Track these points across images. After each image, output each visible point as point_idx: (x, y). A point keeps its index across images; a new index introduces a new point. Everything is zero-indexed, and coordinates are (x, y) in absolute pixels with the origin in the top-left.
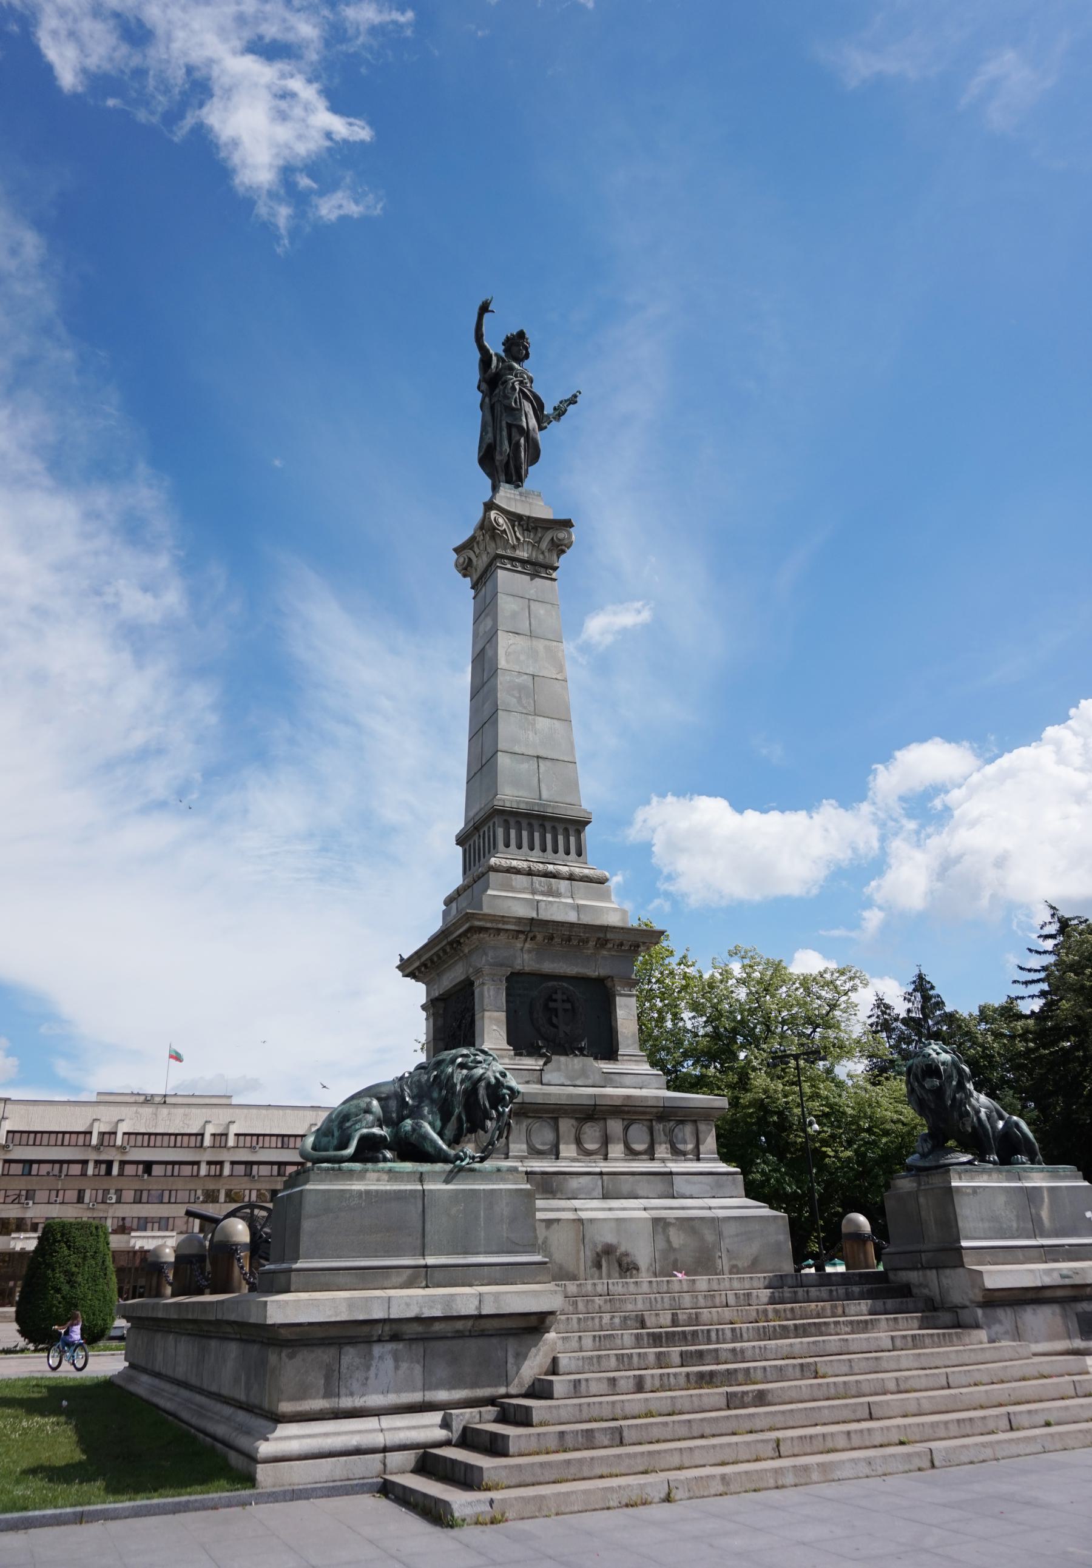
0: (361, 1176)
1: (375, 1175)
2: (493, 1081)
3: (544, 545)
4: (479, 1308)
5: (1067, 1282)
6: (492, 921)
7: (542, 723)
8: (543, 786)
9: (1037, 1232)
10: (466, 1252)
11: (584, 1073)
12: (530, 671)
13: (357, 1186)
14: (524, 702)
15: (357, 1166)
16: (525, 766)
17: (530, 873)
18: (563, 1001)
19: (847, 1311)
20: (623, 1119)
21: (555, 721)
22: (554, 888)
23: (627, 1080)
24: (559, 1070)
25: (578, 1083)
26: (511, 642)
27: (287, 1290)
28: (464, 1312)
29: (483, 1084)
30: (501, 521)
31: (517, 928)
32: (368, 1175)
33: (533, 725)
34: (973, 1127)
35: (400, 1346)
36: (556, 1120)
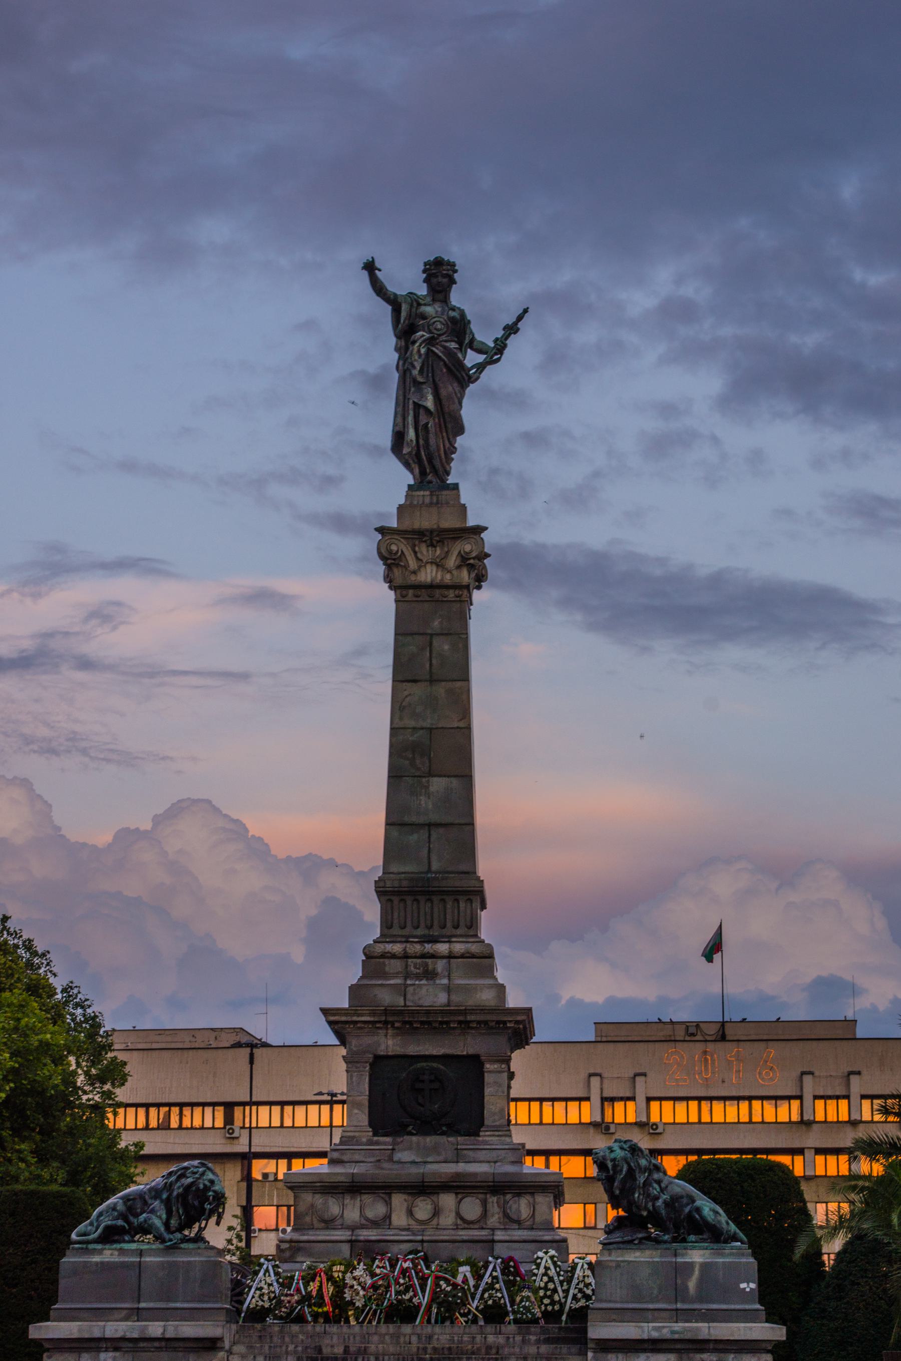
0: (100, 1252)
1: (110, 1252)
2: (201, 1186)
3: (452, 561)
4: (163, 1333)
5: (676, 1336)
6: (340, 1015)
7: (437, 784)
8: (434, 858)
9: (679, 1298)
10: (169, 1300)
11: (435, 1149)
12: (427, 724)
13: (96, 1259)
14: (418, 762)
15: (99, 1246)
16: (415, 837)
17: (406, 956)
18: (431, 1081)
19: (500, 1352)
20: (457, 1194)
21: (452, 779)
22: (430, 967)
23: (481, 1155)
24: (410, 1148)
25: (430, 1159)
26: (406, 693)
27: (48, 1320)
28: (153, 1336)
29: (194, 1188)
30: (394, 548)
31: (372, 1019)
32: (105, 1252)
33: (427, 787)
34: (649, 1212)
35: (117, 1354)
36: (390, 1195)
